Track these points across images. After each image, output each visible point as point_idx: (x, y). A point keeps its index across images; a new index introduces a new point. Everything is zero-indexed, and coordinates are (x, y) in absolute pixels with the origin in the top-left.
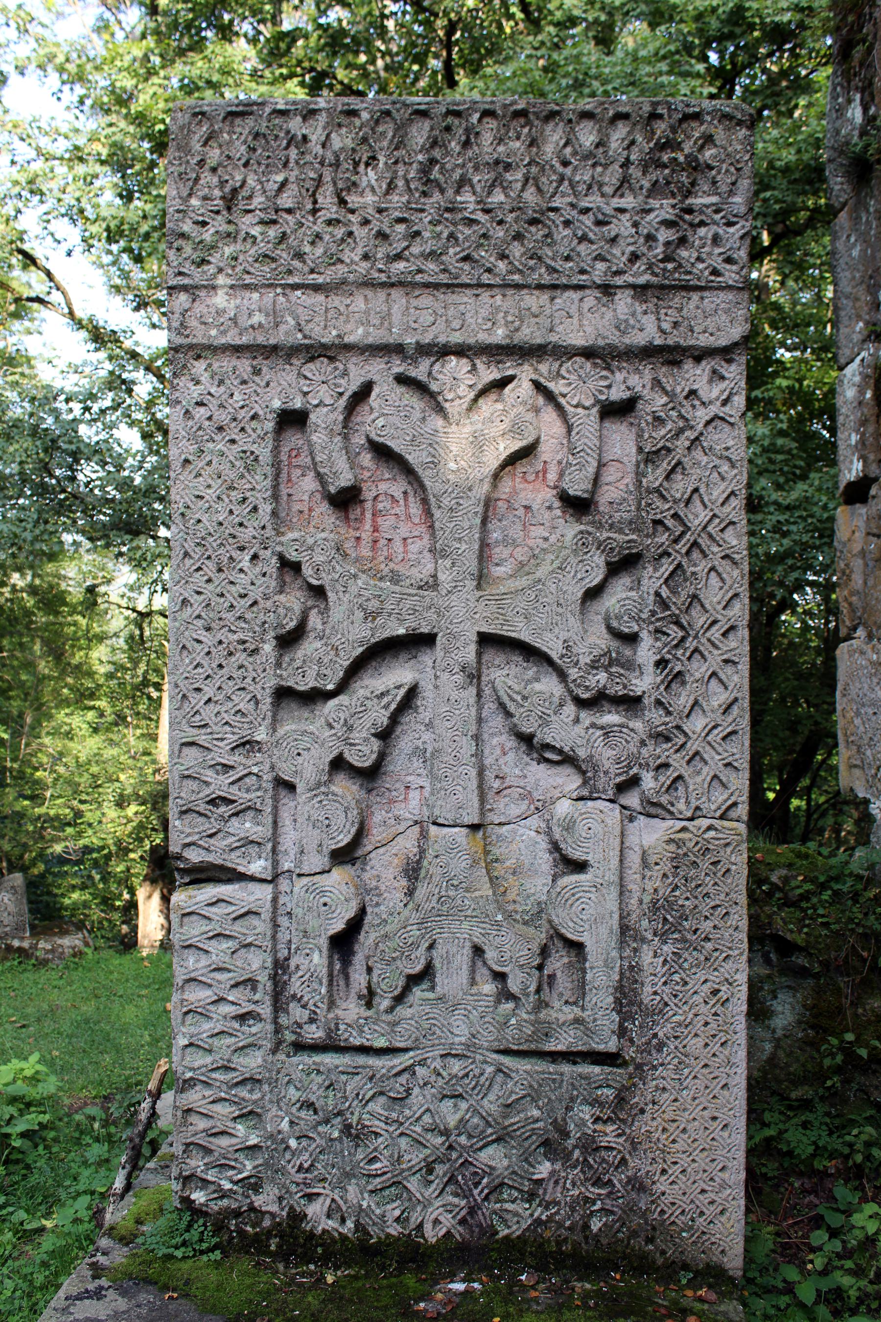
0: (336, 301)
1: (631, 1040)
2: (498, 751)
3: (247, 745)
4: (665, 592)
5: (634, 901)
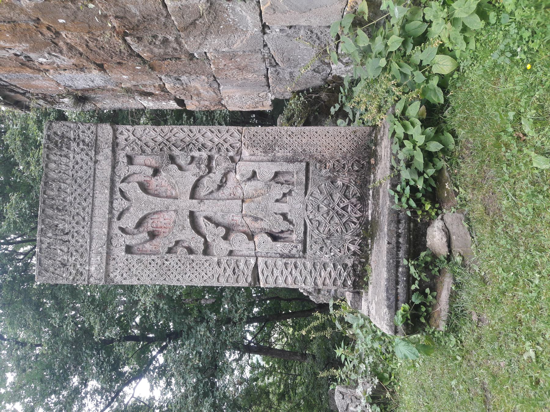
0: (95, 236)
1: (304, 159)
2: (223, 195)
3: (219, 263)
4: (180, 148)
5: (265, 158)
